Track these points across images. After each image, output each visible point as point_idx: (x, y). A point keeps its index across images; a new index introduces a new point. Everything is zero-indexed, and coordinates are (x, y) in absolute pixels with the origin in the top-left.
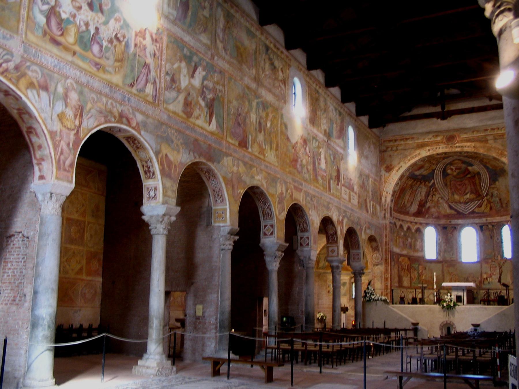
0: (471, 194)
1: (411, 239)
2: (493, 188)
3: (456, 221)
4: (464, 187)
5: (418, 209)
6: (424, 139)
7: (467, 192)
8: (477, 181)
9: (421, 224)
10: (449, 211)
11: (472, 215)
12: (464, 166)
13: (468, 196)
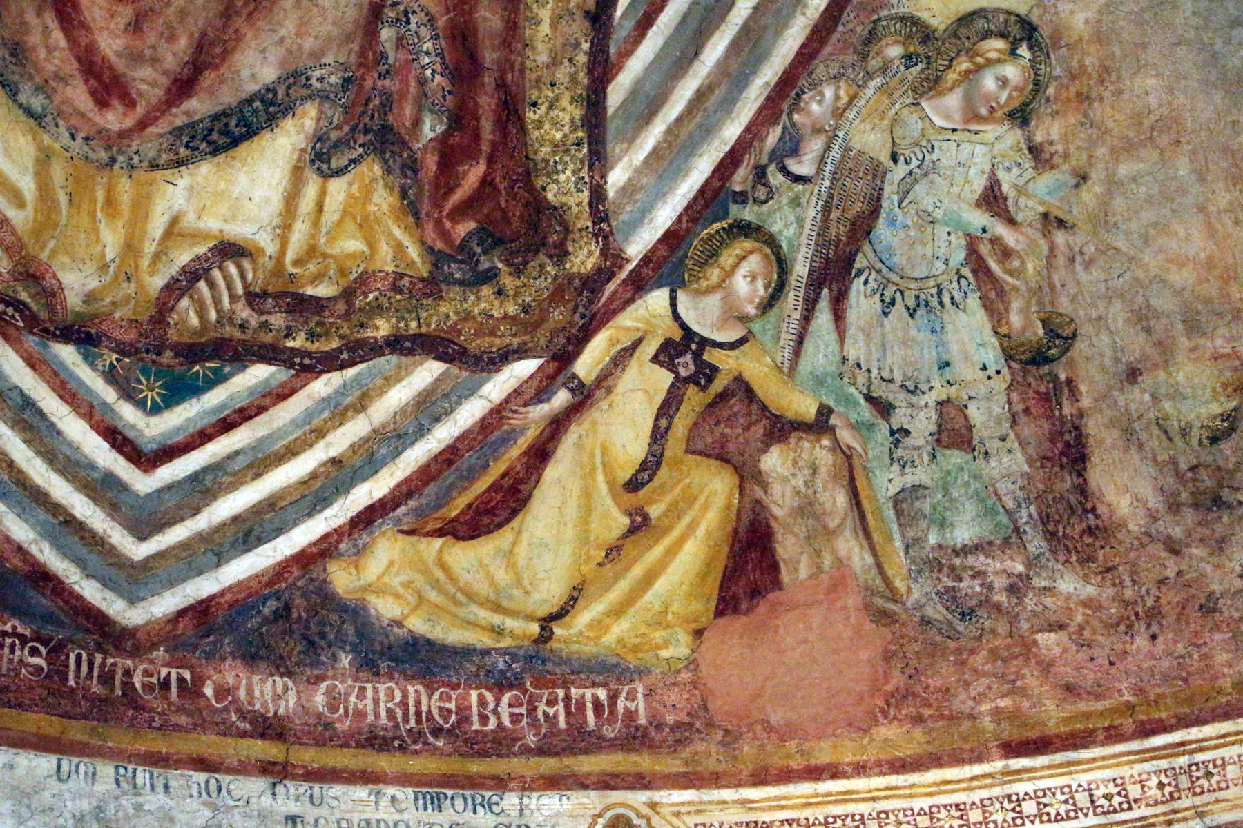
0: (322, 157)
7: (256, 66)
11: (268, 692)
13: (248, 193)
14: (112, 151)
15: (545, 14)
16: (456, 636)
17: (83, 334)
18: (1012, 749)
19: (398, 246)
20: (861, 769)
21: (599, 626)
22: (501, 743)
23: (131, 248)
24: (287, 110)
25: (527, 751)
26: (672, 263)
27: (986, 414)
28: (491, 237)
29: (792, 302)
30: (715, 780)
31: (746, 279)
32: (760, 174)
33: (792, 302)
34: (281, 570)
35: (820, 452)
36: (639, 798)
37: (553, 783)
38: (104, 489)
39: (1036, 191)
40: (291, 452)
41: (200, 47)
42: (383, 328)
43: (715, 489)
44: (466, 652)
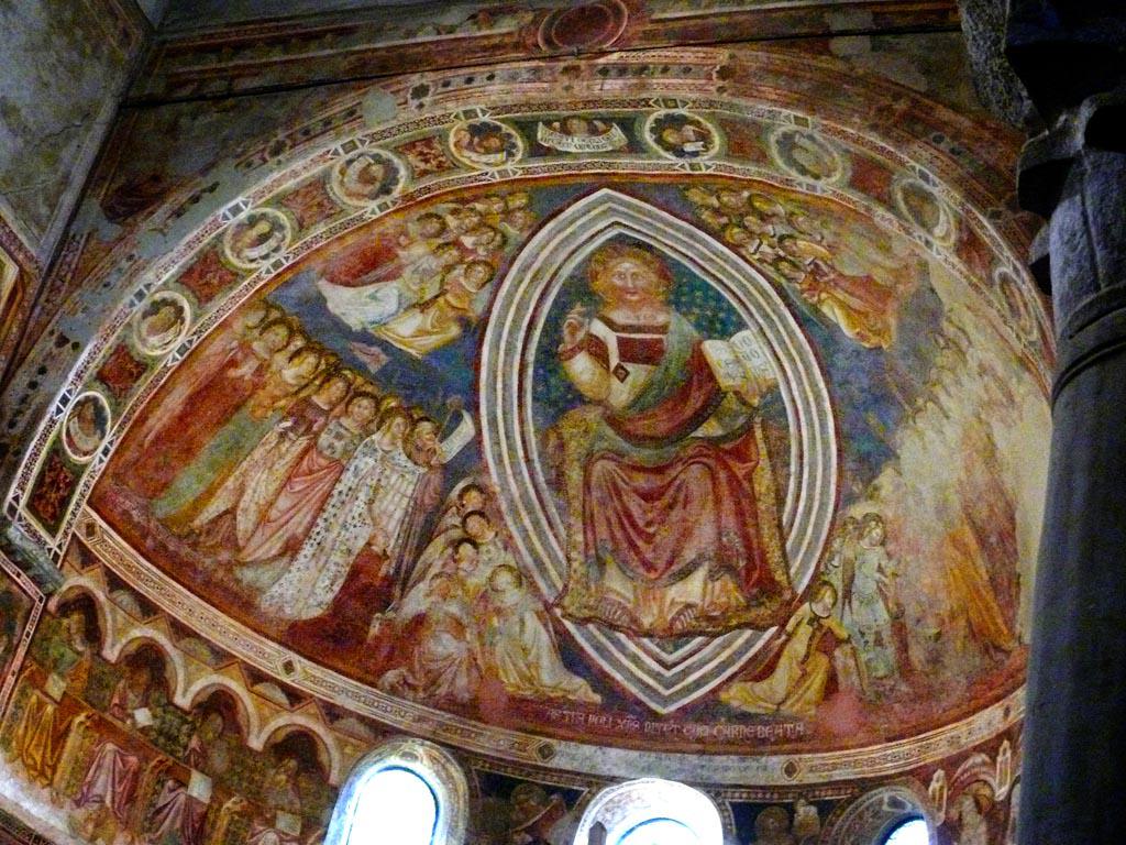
0: (712, 576)
1: (221, 787)
2: (861, 526)
3: (587, 750)
4: (675, 515)
5: (338, 605)
6: (411, 34)
7: (690, 554)
8: (763, 482)
9: (332, 713)
10: (551, 676)
11: (702, 730)
12: (678, 330)
13: (693, 589)
14: (651, 586)
15: (766, 527)
16: (752, 710)
17: (649, 634)
18: (889, 740)
19: (738, 598)
20: (853, 747)
21: (793, 705)
22: (764, 741)
23: (661, 611)
24: (700, 565)
25: (772, 744)
26: (811, 594)
27: (886, 635)
28: (763, 592)
29: (839, 604)
30: (817, 751)
31: (828, 598)
32: (826, 567)
33: (839, 604)
34: (706, 695)
35: (847, 648)
36: (797, 757)
37: (775, 753)
38: (657, 676)
39: (890, 567)
40: (711, 660)
41: (673, 552)
42: (734, 622)
43: (823, 661)
44: (757, 715)
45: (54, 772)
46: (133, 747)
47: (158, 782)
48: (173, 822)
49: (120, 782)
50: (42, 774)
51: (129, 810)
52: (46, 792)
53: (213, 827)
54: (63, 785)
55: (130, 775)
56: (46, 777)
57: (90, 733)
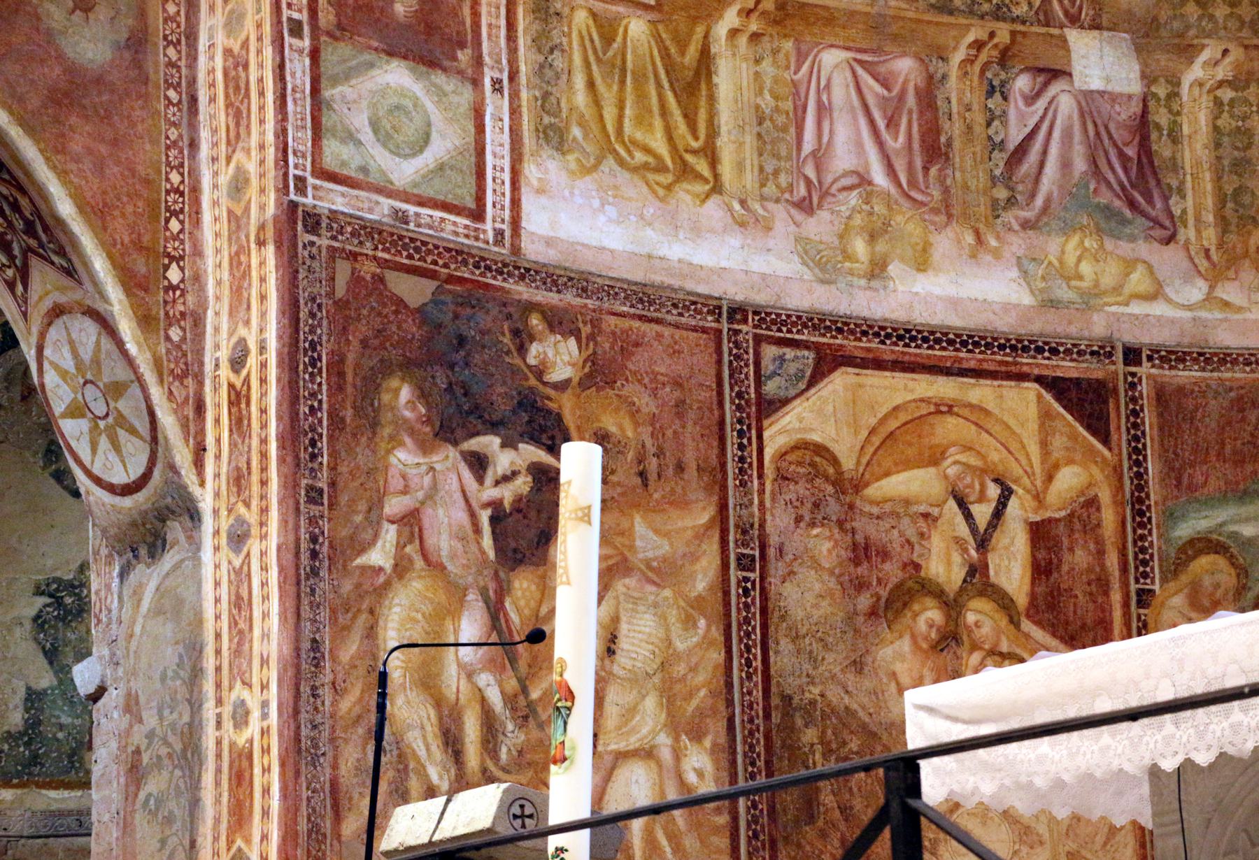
45: (714, 162)
46: (895, 38)
47: (991, 92)
48: (1066, 165)
49: (892, 123)
50: (685, 172)
51: (942, 180)
52: (713, 210)
53: (1175, 137)
54: (750, 179)
55: (911, 101)
56: (699, 177)
57: (766, 43)
